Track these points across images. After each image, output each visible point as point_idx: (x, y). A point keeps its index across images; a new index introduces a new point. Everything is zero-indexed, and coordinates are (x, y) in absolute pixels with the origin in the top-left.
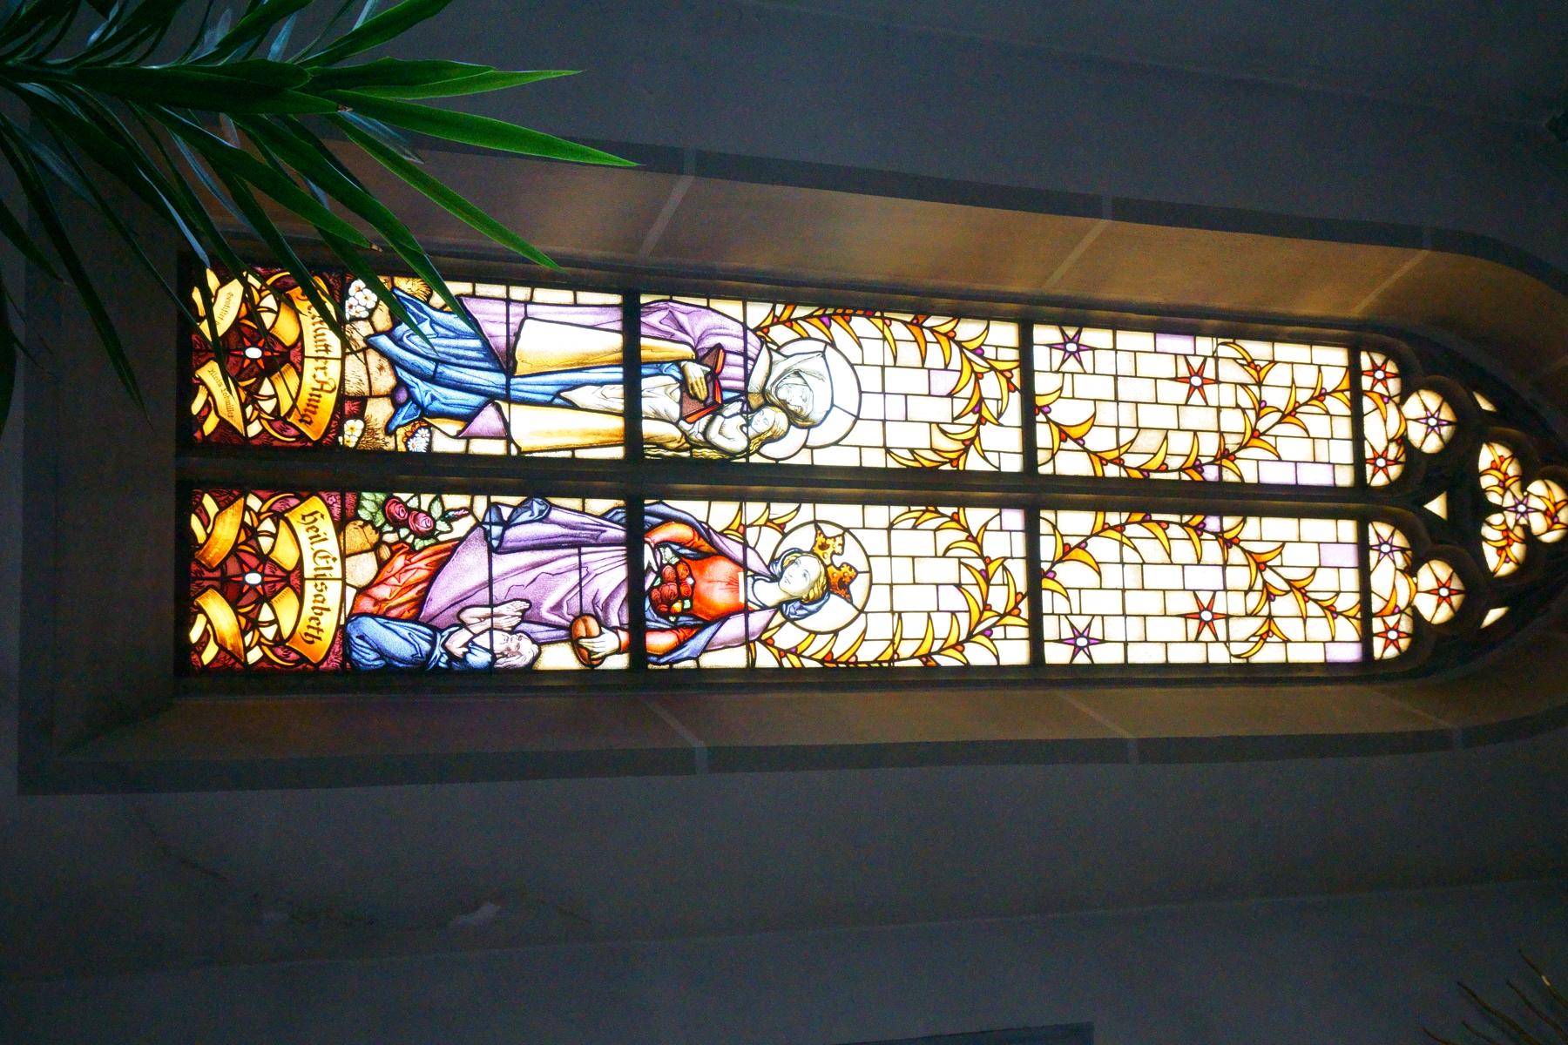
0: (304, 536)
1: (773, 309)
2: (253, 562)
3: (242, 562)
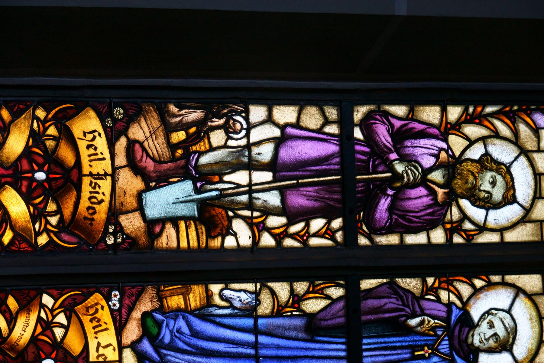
0: (89, 326)
1: (466, 110)
2: (47, 349)
3: (39, 349)
